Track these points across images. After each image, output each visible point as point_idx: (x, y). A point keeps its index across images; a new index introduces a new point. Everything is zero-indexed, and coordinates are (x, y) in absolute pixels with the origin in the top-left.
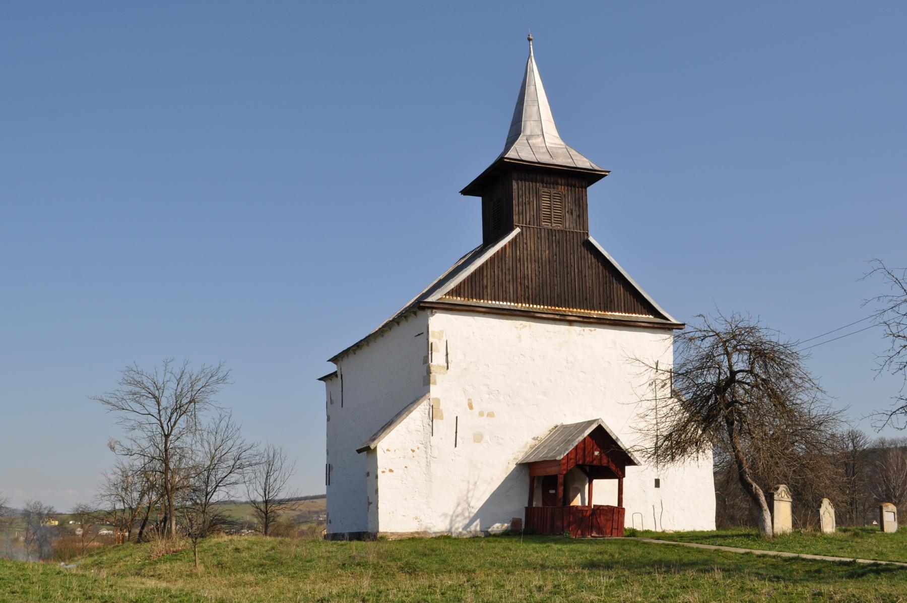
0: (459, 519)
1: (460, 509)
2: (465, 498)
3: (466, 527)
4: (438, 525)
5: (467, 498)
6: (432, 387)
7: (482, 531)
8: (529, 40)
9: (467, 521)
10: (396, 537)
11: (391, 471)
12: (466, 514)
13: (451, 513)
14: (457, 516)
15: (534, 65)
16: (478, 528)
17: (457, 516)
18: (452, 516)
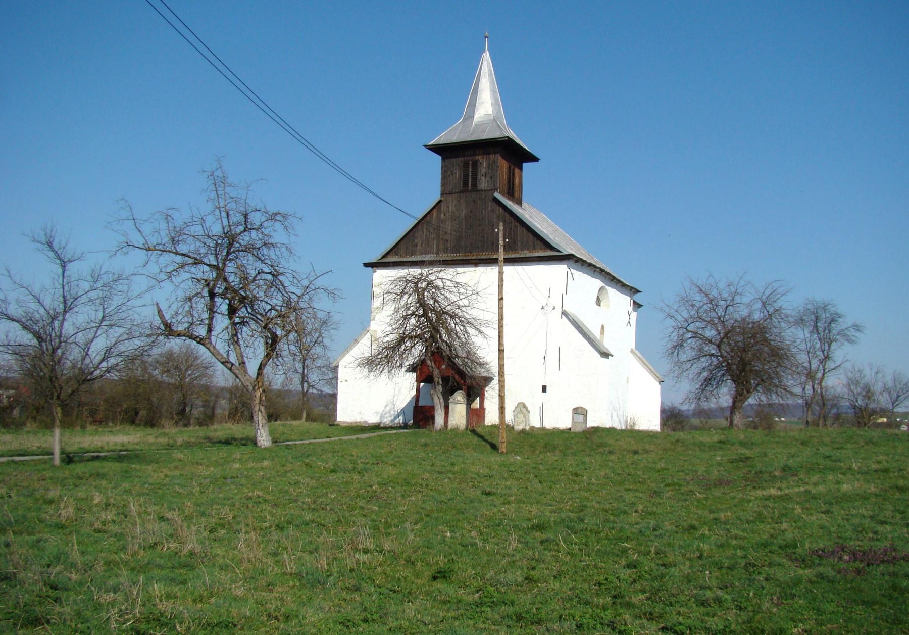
0: (386, 416)
1: (388, 408)
2: (392, 401)
3: (392, 421)
4: (372, 419)
5: (394, 401)
6: (372, 323)
7: (403, 423)
8: (486, 37)
9: (393, 418)
10: (345, 425)
11: (346, 381)
12: (392, 413)
13: (381, 412)
14: (386, 414)
15: (486, 56)
16: (401, 422)
17: (386, 414)
18: (382, 414)
